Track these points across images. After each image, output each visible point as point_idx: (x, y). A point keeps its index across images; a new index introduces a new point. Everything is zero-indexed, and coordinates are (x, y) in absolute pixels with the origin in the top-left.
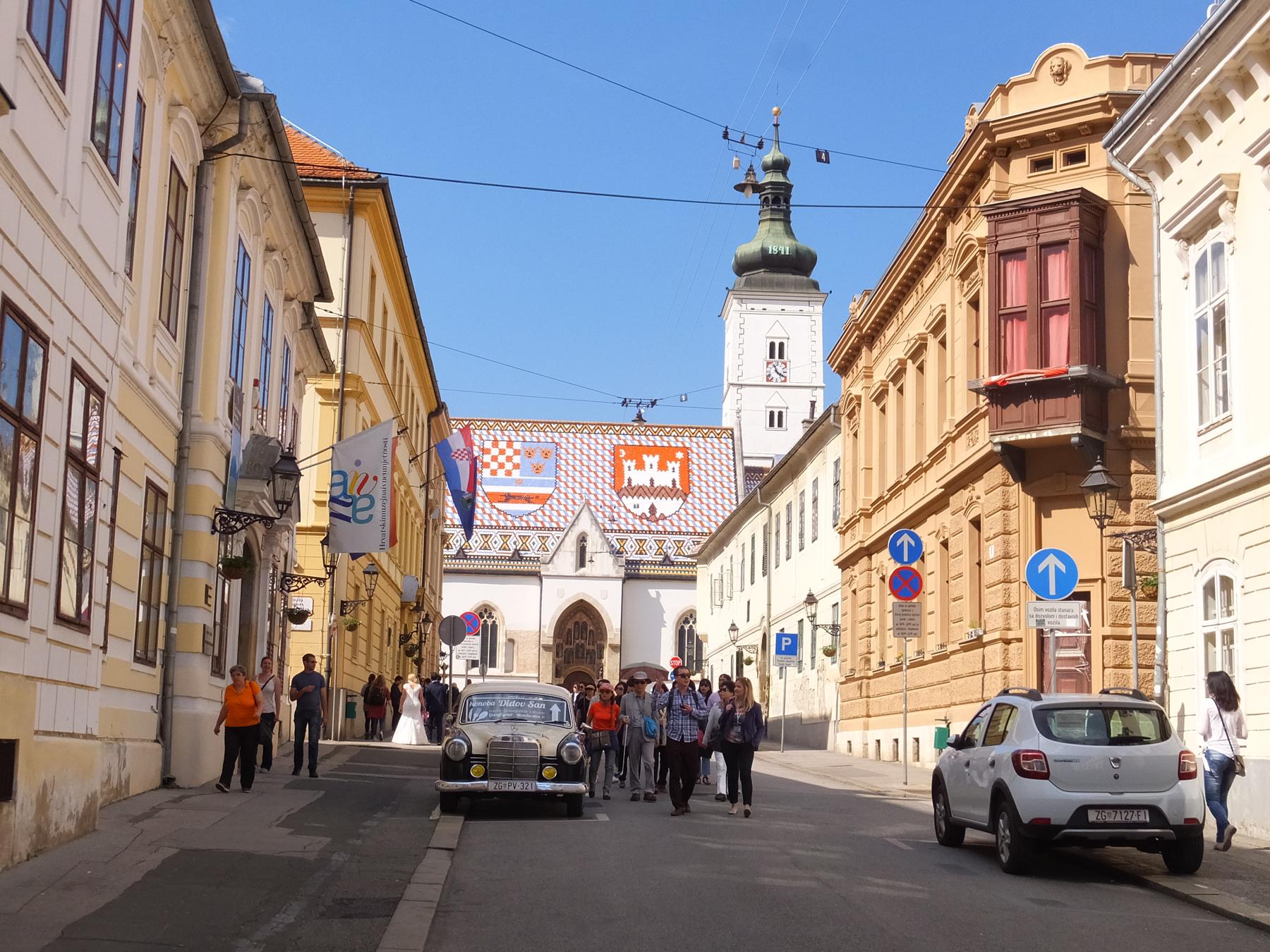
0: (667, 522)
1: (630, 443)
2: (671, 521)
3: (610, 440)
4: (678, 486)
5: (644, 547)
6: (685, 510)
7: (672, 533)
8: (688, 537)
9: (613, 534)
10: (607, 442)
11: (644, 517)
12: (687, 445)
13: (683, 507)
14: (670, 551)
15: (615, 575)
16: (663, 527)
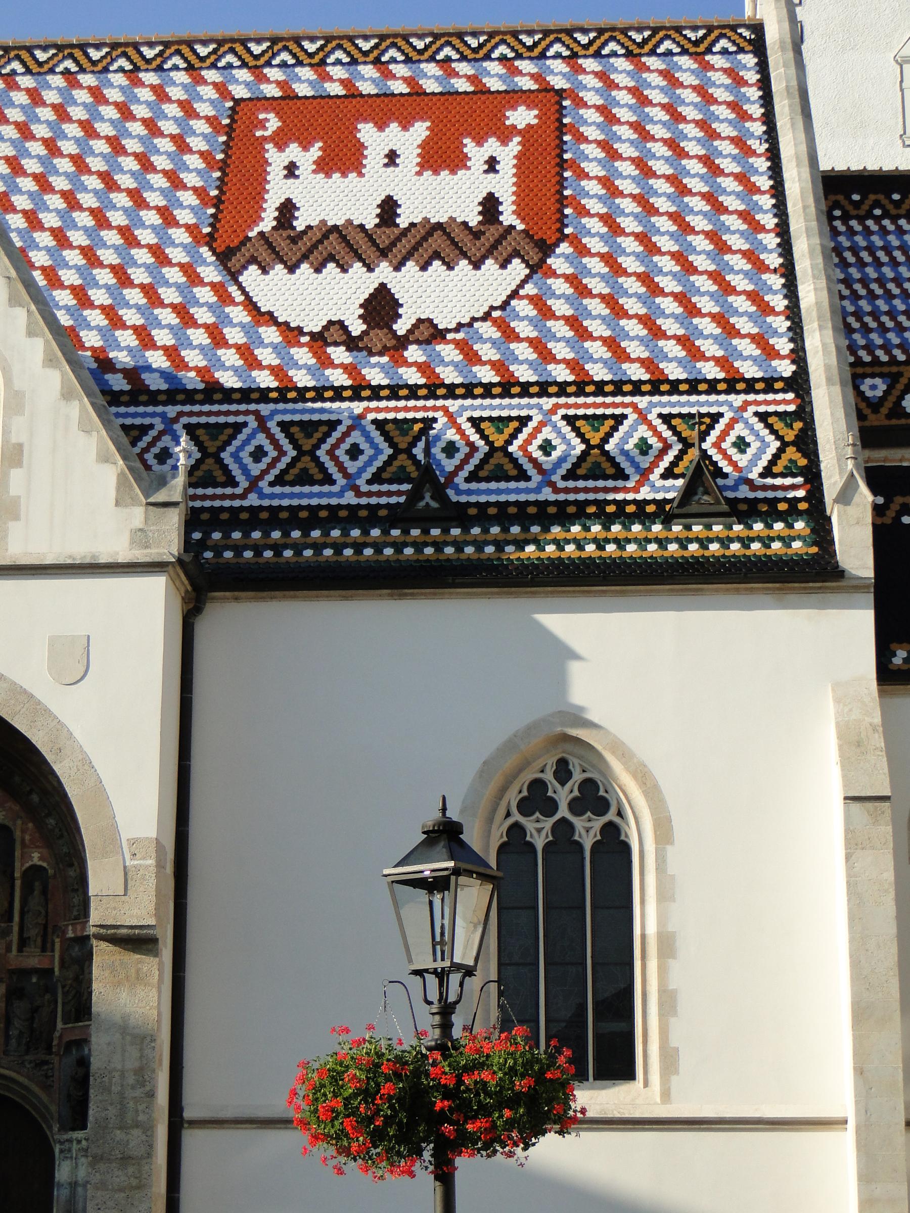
0: (448, 351)
1: (303, 90)
2: (464, 347)
3: (222, 89)
4: (508, 217)
5: (321, 453)
6: (538, 301)
7: (469, 390)
8: (547, 403)
9: (171, 411)
10: (208, 92)
11: (335, 334)
12: (558, 83)
13: (530, 289)
14: (449, 465)
15: (124, 555)
16: (424, 368)
